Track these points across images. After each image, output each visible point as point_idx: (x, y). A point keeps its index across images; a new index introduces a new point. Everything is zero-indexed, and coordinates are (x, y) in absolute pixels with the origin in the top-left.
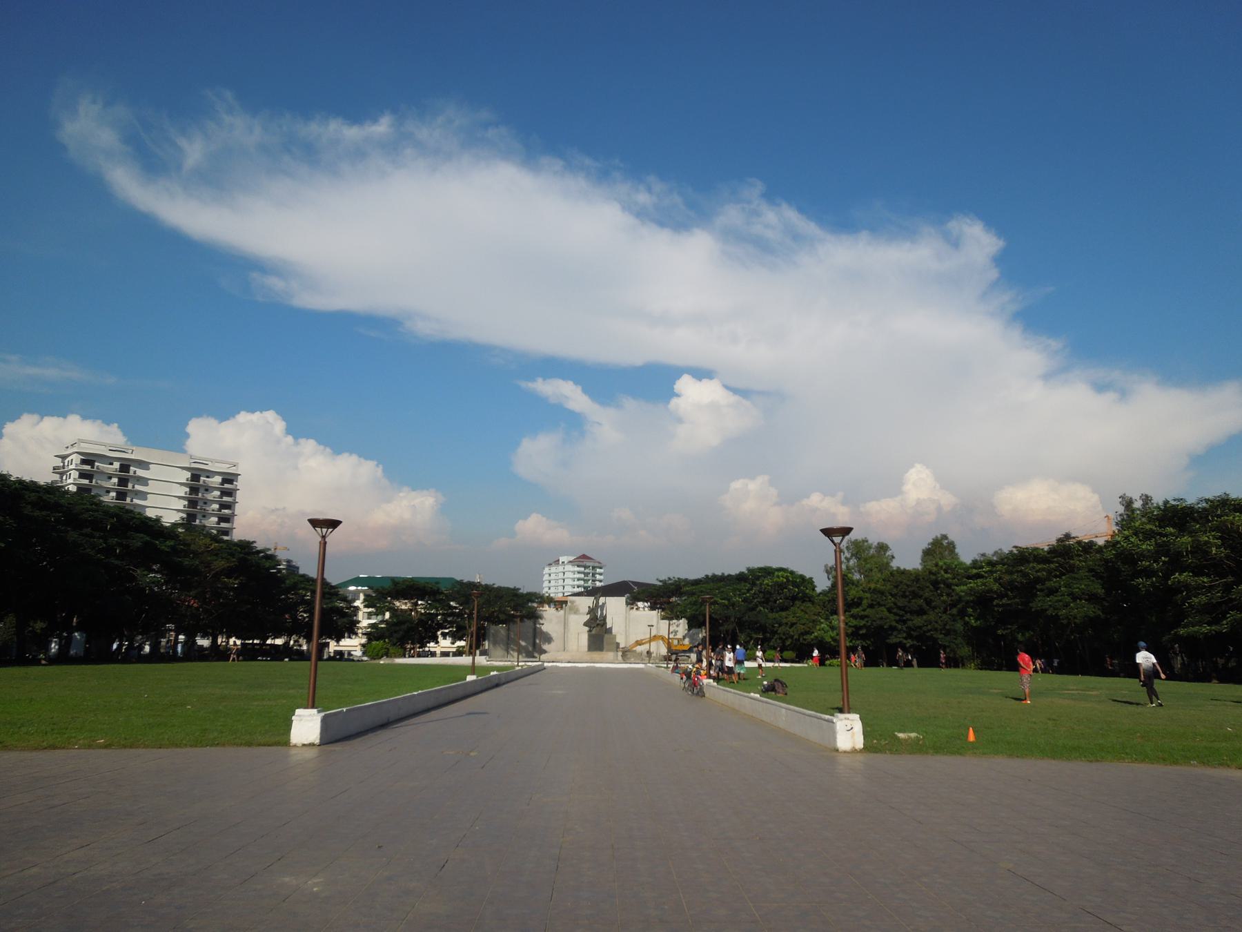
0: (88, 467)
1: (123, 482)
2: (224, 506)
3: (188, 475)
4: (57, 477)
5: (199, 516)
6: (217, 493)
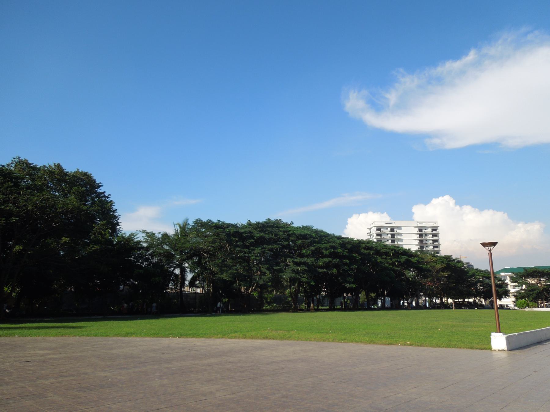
0: (379, 232)
1: (393, 236)
2: (434, 241)
3: (417, 229)
4: (369, 237)
5: (425, 246)
6: (431, 236)
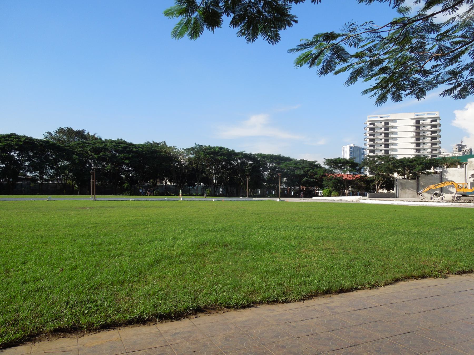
0: (372, 126)
1: (387, 129)
3: (414, 121)
5: (421, 138)
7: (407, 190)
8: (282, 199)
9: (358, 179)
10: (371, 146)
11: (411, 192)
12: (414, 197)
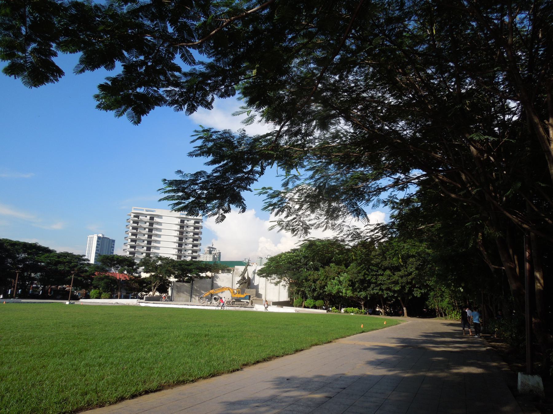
0: (137, 219)
1: (151, 224)
2: (195, 234)
3: (179, 220)
5: (184, 238)
7: (182, 294)
8: (72, 301)
9: (132, 280)
10: (132, 240)
11: (185, 296)
12: (187, 301)
